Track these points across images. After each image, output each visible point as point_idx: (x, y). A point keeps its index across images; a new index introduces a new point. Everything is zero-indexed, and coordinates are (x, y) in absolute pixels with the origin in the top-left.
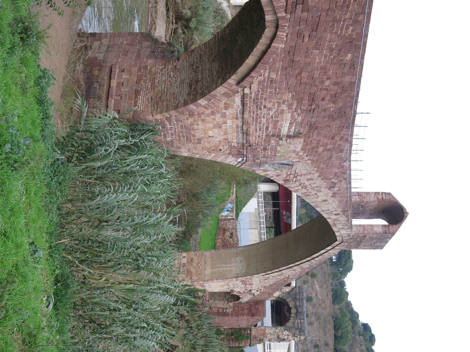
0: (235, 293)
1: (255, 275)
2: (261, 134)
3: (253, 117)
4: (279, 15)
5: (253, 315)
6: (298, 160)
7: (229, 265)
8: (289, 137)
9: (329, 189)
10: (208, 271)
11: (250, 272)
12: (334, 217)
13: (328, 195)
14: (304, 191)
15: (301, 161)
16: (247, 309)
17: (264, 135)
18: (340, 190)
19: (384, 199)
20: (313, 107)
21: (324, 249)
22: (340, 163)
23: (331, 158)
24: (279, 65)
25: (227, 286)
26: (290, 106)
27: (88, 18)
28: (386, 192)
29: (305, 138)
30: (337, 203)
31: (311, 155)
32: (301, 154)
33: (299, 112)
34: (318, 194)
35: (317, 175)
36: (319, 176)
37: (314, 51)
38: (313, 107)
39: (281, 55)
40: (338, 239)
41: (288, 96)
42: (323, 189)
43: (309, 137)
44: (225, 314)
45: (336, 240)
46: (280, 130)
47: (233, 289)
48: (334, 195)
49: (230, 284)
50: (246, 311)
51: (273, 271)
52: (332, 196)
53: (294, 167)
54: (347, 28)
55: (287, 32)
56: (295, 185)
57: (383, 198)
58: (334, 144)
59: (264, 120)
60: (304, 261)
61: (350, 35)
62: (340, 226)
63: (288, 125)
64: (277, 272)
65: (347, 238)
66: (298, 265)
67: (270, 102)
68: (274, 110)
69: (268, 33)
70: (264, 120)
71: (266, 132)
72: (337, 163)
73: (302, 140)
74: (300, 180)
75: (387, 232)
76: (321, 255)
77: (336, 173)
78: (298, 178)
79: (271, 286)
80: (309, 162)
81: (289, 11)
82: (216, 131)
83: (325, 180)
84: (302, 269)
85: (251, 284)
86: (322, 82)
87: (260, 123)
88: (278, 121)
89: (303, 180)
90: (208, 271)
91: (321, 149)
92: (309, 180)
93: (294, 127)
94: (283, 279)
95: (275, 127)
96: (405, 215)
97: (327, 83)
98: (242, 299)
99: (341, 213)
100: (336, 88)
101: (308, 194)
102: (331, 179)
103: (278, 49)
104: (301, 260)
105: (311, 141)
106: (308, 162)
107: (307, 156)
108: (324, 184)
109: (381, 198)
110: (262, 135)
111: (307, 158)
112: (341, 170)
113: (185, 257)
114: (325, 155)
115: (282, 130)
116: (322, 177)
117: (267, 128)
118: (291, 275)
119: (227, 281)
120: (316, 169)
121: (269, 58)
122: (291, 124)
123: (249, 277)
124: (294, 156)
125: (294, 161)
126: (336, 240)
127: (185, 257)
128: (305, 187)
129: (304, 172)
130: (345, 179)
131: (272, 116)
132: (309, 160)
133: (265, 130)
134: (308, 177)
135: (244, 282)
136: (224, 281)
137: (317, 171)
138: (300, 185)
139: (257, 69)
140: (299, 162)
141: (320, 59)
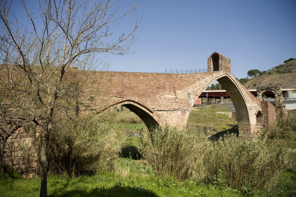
7: (243, 115)
8: (176, 95)
18: (200, 76)
20: (162, 87)
22: (188, 77)
23: (185, 81)
24: (145, 99)
26: (161, 95)
30: (207, 77)
35: (193, 85)
36: (194, 84)
37: (139, 88)
38: (162, 87)
41: (157, 96)
42: (200, 82)
46: (173, 98)
51: (244, 99)
53: (190, 93)
54: (130, 79)
59: (168, 104)
60: (238, 87)
63: (170, 96)
67: (160, 102)
68: (163, 100)
70: (168, 104)
72: (187, 78)
73: (177, 91)
77: (192, 78)
79: (252, 99)
80: (187, 88)
81: (123, 97)
82: (173, 120)
86: (152, 85)
91: (181, 84)
95: (171, 100)
99: (212, 75)
104: (238, 89)
111: (186, 89)
114: (184, 82)
117: (172, 102)
122: (170, 95)
124: (184, 93)
130: (195, 75)
132: (186, 88)
134: (194, 88)
135: (251, 109)
139: (146, 106)
140: (187, 91)
141: (142, 86)
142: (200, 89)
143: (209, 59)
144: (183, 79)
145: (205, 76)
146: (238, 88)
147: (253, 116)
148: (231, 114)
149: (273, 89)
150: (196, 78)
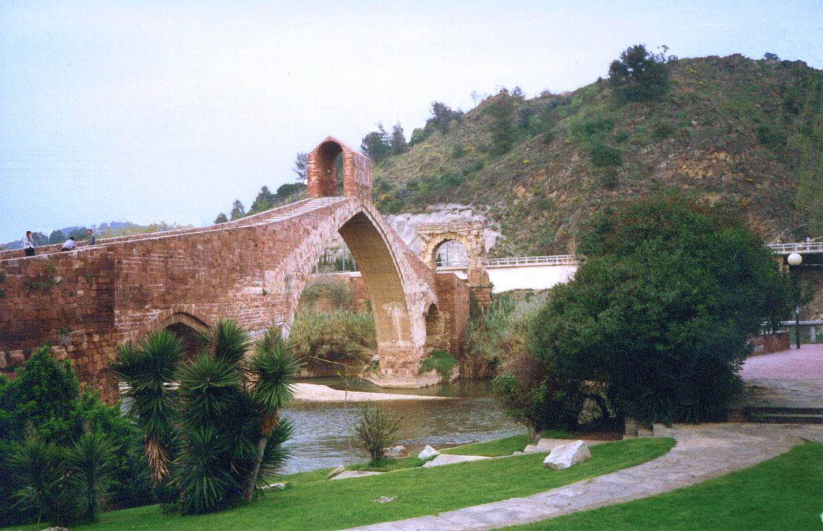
0: (427, 311)
3: (249, 321)
4: (172, 313)
5: (453, 288)
6: (283, 271)
9: (309, 234)
10: (401, 343)
11: (401, 299)
12: (337, 222)
14: (312, 258)
18: (310, 224)
20: (238, 267)
26: (238, 290)
32: (277, 270)
35: (297, 250)
36: (298, 247)
38: (238, 267)
39: (200, 306)
41: (231, 294)
42: (310, 241)
44: (452, 321)
45: (362, 212)
48: (315, 228)
49: (415, 318)
50: (448, 295)
51: (398, 272)
52: (316, 229)
54: (180, 254)
57: (314, 164)
58: (269, 240)
59: (251, 311)
60: (385, 241)
61: (185, 250)
62: (347, 213)
65: (359, 201)
66: (390, 246)
69: (185, 321)
71: (260, 306)
72: (285, 233)
73: (266, 272)
77: (295, 231)
78: (300, 267)
79: (416, 271)
84: (395, 241)
85: (415, 294)
87: (252, 314)
88: (251, 298)
89: (301, 262)
90: (401, 343)
91: (274, 252)
102: (300, 235)
103: (195, 310)
104: (385, 244)
105: (267, 263)
107: (279, 264)
108: (305, 240)
111: (281, 263)
113: (386, 371)
115: (258, 292)
117: (257, 307)
119: (412, 322)
121: (202, 315)
123: (406, 298)
126: (362, 212)
127: (386, 371)
131: (247, 304)
134: (299, 257)
136: (412, 325)
137: (293, 250)
142: (309, 258)
146: (387, 244)
149: (465, 234)
150: (302, 229)
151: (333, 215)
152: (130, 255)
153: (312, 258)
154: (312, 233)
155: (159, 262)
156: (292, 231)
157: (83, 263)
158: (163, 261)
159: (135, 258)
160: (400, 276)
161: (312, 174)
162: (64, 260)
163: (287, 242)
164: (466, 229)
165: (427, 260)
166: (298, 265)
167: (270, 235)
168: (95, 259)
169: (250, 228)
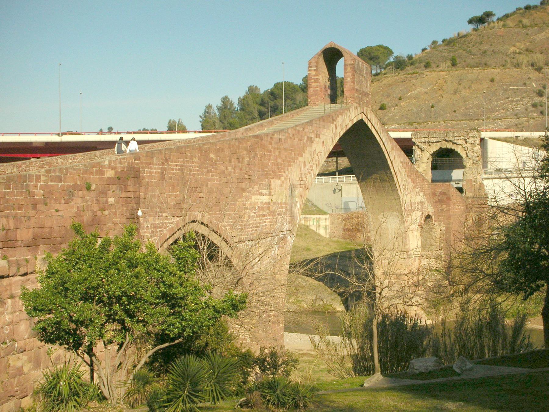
1: (400, 201)
2: (269, 220)
6: (288, 180)
9: (312, 142)
13: (318, 142)
14: (315, 167)
15: (289, 177)
16: (442, 206)
17: (269, 217)
19: (315, 68)
20: (247, 176)
21: (370, 130)
25: (414, 231)
27: (115, 398)
28: (308, 65)
29: (270, 178)
30: (325, 130)
31: (284, 169)
32: (283, 178)
33: (250, 189)
34: (317, 152)
36: (302, 156)
38: (247, 176)
40: (360, 119)
42: (313, 149)
43: (270, 175)
45: (361, 121)
46: (266, 203)
47: (417, 224)
48: (318, 136)
50: (444, 206)
52: (319, 138)
55: (197, 212)
56: (310, 178)
57: (315, 70)
58: (275, 148)
64: (397, 177)
65: (359, 109)
72: (289, 141)
73: (272, 181)
74: (305, 174)
75: (352, 66)
76: (377, 132)
77: (299, 140)
83: (305, 149)
84: (393, 149)
87: (260, 223)
91: (279, 161)
92: (305, 165)
93: (262, 191)
94: (405, 168)
96: (333, 46)
97: (230, 169)
98: (429, 212)
100: (233, 160)
101: (317, 163)
102: (304, 143)
105: (273, 172)
106: (289, 170)
107: (285, 173)
109: (315, 72)
110: (269, 219)
111: (287, 172)
112: (295, 136)
115: (264, 201)
116: (303, 153)
118: (400, 160)
120: (295, 161)
121: (214, 223)
123: (403, 208)
125: (289, 184)
128: (311, 167)
129: (298, 173)
130: (303, 130)
131: (255, 213)
133: (265, 218)
135: (410, 213)
137: (297, 159)
138: (309, 173)
140: (289, 179)
143: (314, 64)
144: (282, 147)
145: (322, 129)
147: (415, 233)
148: (328, 223)
149: (460, 142)
150: (306, 137)
151: (335, 123)
152: (150, 164)
153: (315, 167)
154: (314, 142)
155: (176, 170)
156: (297, 139)
157: (113, 171)
158: (179, 170)
159: (155, 166)
160: (397, 185)
161: (313, 81)
162: (97, 169)
163: (291, 150)
164: (462, 137)
165: (511, 179)
166: (301, 174)
167: (276, 143)
168: (124, 168)
169: (257, 136)
